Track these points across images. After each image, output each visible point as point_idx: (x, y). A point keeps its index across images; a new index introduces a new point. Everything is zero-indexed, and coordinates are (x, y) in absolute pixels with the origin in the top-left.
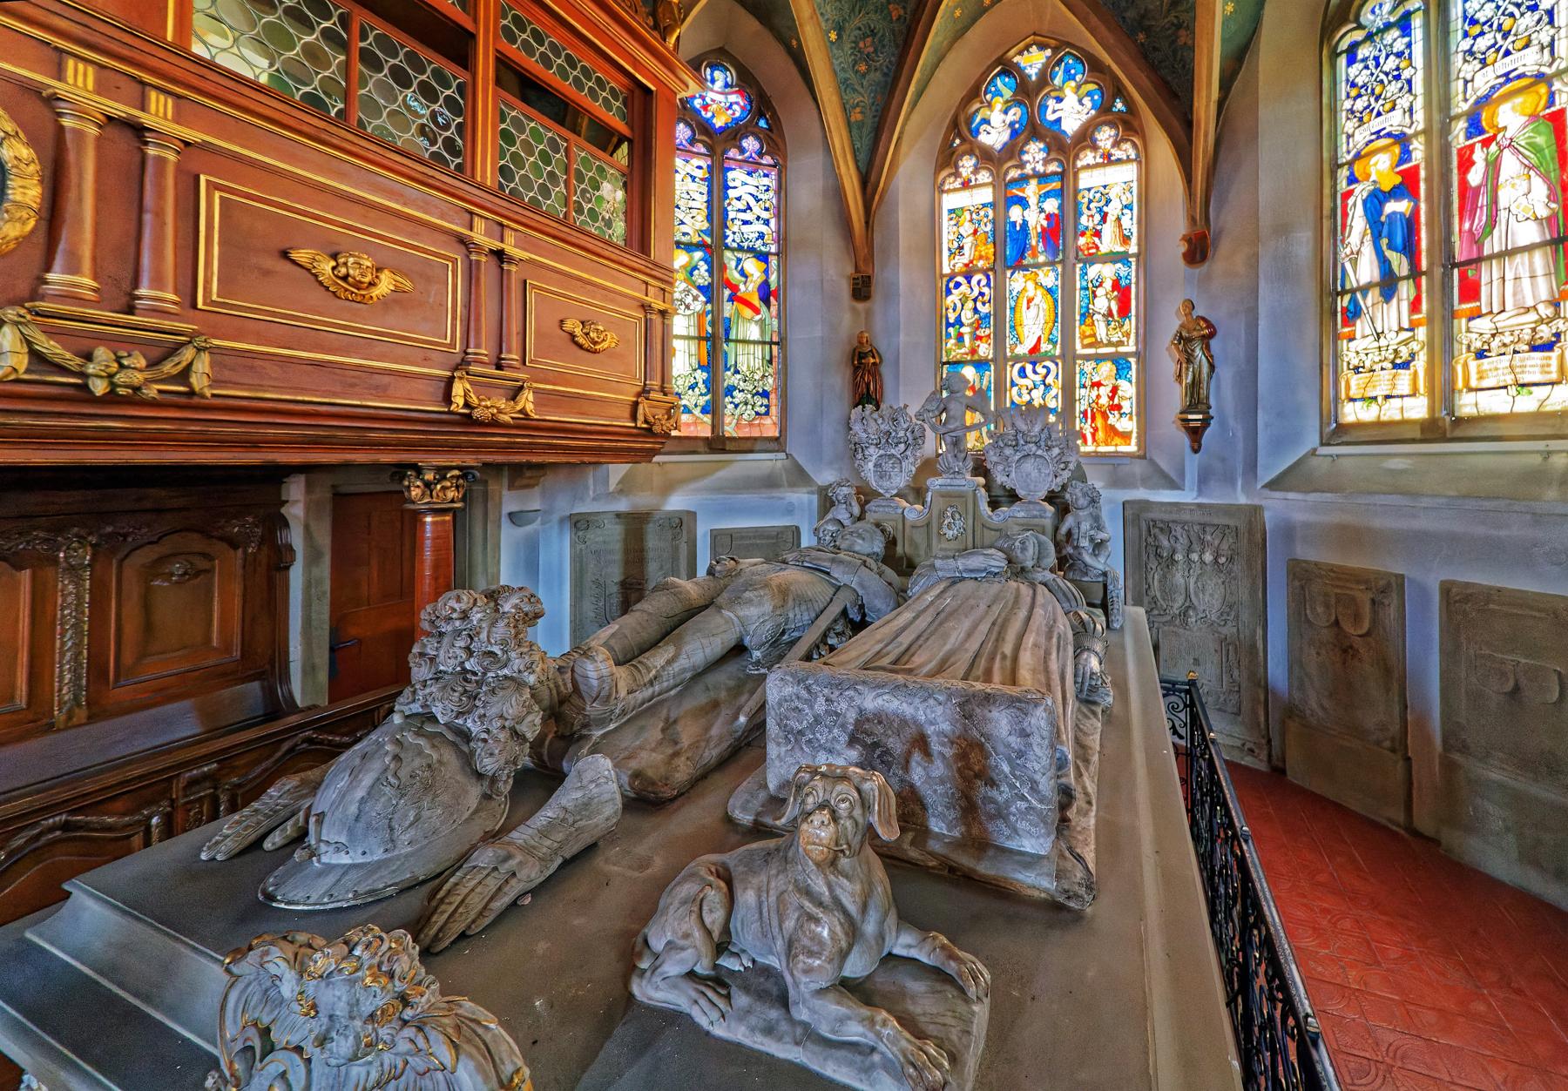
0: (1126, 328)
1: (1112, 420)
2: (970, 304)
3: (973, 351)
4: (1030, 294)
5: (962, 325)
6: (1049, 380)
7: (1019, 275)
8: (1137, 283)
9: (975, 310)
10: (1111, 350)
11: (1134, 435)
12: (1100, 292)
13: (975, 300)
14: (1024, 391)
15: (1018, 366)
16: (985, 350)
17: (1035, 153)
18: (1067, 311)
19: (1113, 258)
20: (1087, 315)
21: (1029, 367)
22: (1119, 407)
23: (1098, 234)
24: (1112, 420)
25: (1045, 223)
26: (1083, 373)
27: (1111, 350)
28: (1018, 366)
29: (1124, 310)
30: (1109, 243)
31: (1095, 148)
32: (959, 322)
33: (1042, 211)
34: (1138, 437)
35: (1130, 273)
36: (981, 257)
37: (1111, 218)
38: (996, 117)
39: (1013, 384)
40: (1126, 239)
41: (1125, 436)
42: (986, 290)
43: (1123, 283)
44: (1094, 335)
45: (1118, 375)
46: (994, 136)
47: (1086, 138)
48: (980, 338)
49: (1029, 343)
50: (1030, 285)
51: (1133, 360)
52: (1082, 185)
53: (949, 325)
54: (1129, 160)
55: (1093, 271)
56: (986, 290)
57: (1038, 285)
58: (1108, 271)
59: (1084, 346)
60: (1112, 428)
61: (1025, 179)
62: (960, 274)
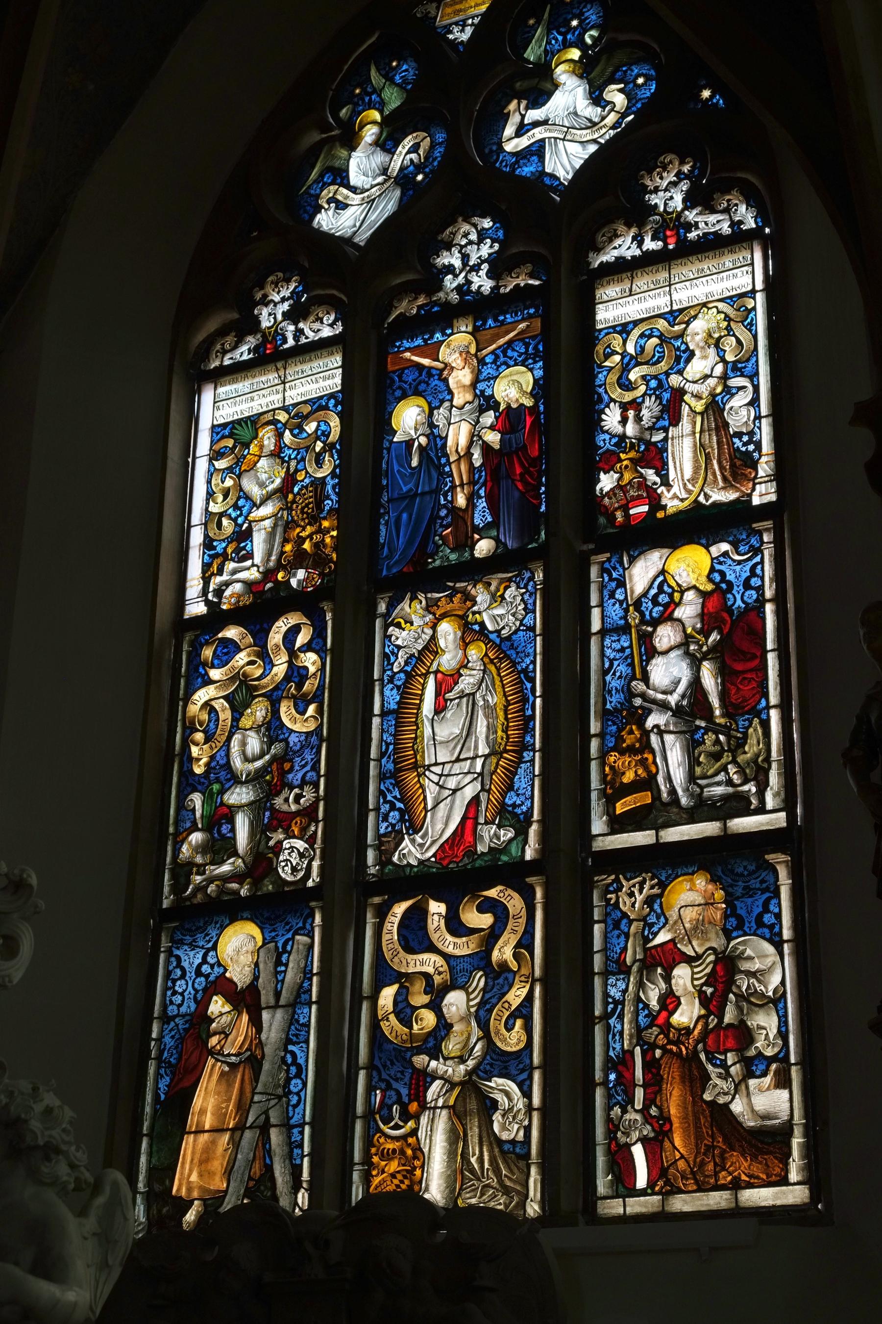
0: (752, 748)
1: (717, 1088)
2: (259, 711)
3: (262, 861)
4: (448, 661)
5: (235, 779)
6: (504, 952)
7: (413, 609)
8: (779, 599)
9: (273, 729)
10: (708, 828)
11: (797, 1141)
12: (666, 636)
13: (274, 699)
14: (419, 999)
15: (400, 909)
16: (296, 858)
17: (469, 257)
18: (566, 712)
19: (696, 525)
20: (630, 714)
21: (436, 908)
22: (744, 1035)
23: (655, 456)
24: (717, 1088)
25: (493, 438)
26: (616, 921)
27: (708, 828)
28: (400, 909)
29: (743, 701)
30: (685, 478)
31: (638, 214)
32: (222, 773)
33: (487, 403)
34: (809, 1150)
35: (757, 570)
36: (299, 559)
37: (693, 404)
38: (362, 165)
39: (384, 973)
40: (740, 466)
41: (769, 1141)
42: (310, 660)
43: (738, 600)
44: (648, 783)
45: (735, 923)
46: (357, 201)
47: (613, 183)
48: (282, 821)
49: (442, 823)
50: (447, 631)
51: (781, 865)
52: (607, 314)
53: (189, 783)
54: (739, 238)
55: (642, 574)
56: (310, 660)
57: (472, 631)
58: (690, 565)
59: (617, 825)
60: (721, 1114)
61: (443, 318)
62: (236, 616)
